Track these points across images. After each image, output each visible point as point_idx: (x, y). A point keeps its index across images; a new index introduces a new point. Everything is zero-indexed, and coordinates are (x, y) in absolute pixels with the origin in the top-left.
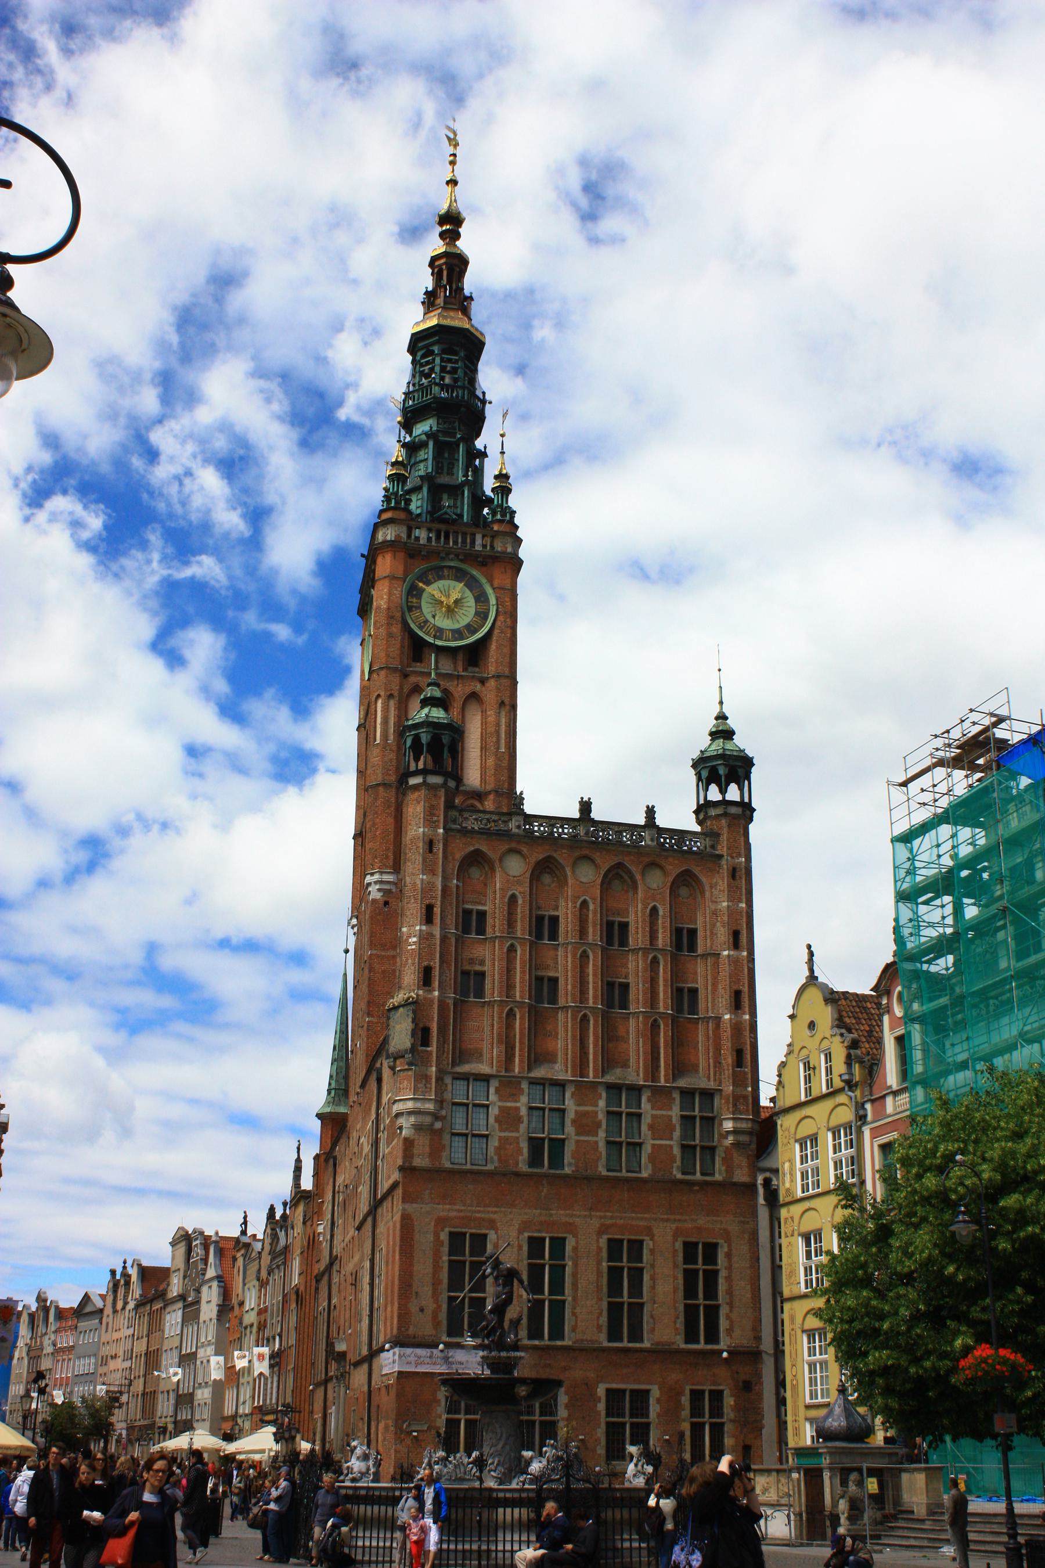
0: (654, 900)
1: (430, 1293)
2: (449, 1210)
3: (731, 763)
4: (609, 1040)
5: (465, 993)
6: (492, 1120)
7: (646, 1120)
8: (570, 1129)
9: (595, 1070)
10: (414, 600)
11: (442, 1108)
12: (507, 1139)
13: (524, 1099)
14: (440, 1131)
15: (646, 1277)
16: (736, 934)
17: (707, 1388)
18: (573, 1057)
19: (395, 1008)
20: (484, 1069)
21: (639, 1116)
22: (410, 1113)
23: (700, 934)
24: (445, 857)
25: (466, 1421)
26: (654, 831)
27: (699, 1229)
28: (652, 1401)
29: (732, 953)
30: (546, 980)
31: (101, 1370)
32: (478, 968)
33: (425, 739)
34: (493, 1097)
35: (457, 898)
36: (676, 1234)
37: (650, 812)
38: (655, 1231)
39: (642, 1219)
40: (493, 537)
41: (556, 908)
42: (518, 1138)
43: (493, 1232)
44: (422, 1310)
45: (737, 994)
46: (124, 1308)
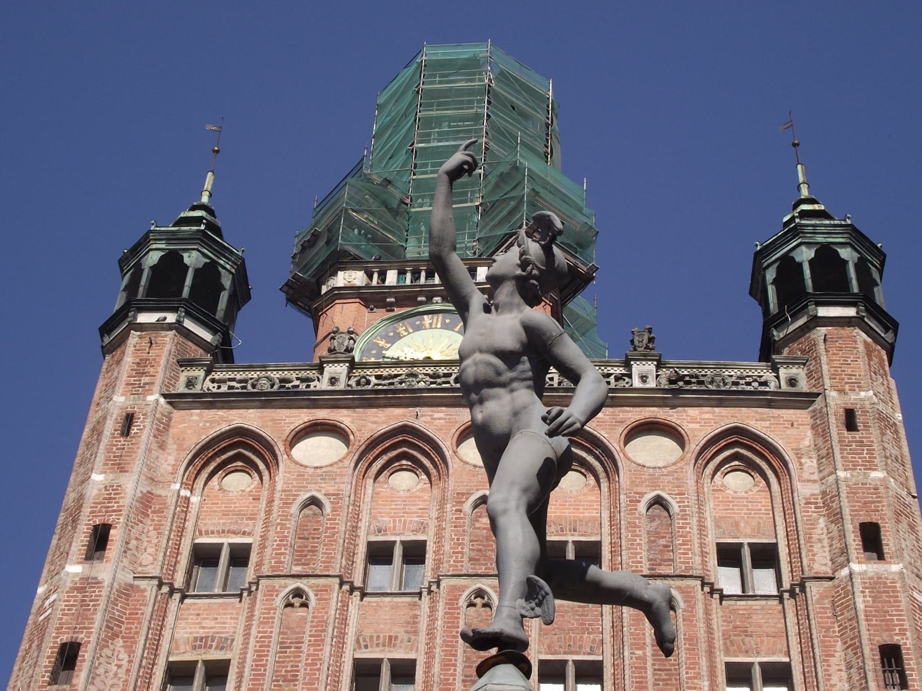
0: (655, 486)
3: (820, 239)
29: (861, 567)
32: (215, 655)
41: (423, 528)
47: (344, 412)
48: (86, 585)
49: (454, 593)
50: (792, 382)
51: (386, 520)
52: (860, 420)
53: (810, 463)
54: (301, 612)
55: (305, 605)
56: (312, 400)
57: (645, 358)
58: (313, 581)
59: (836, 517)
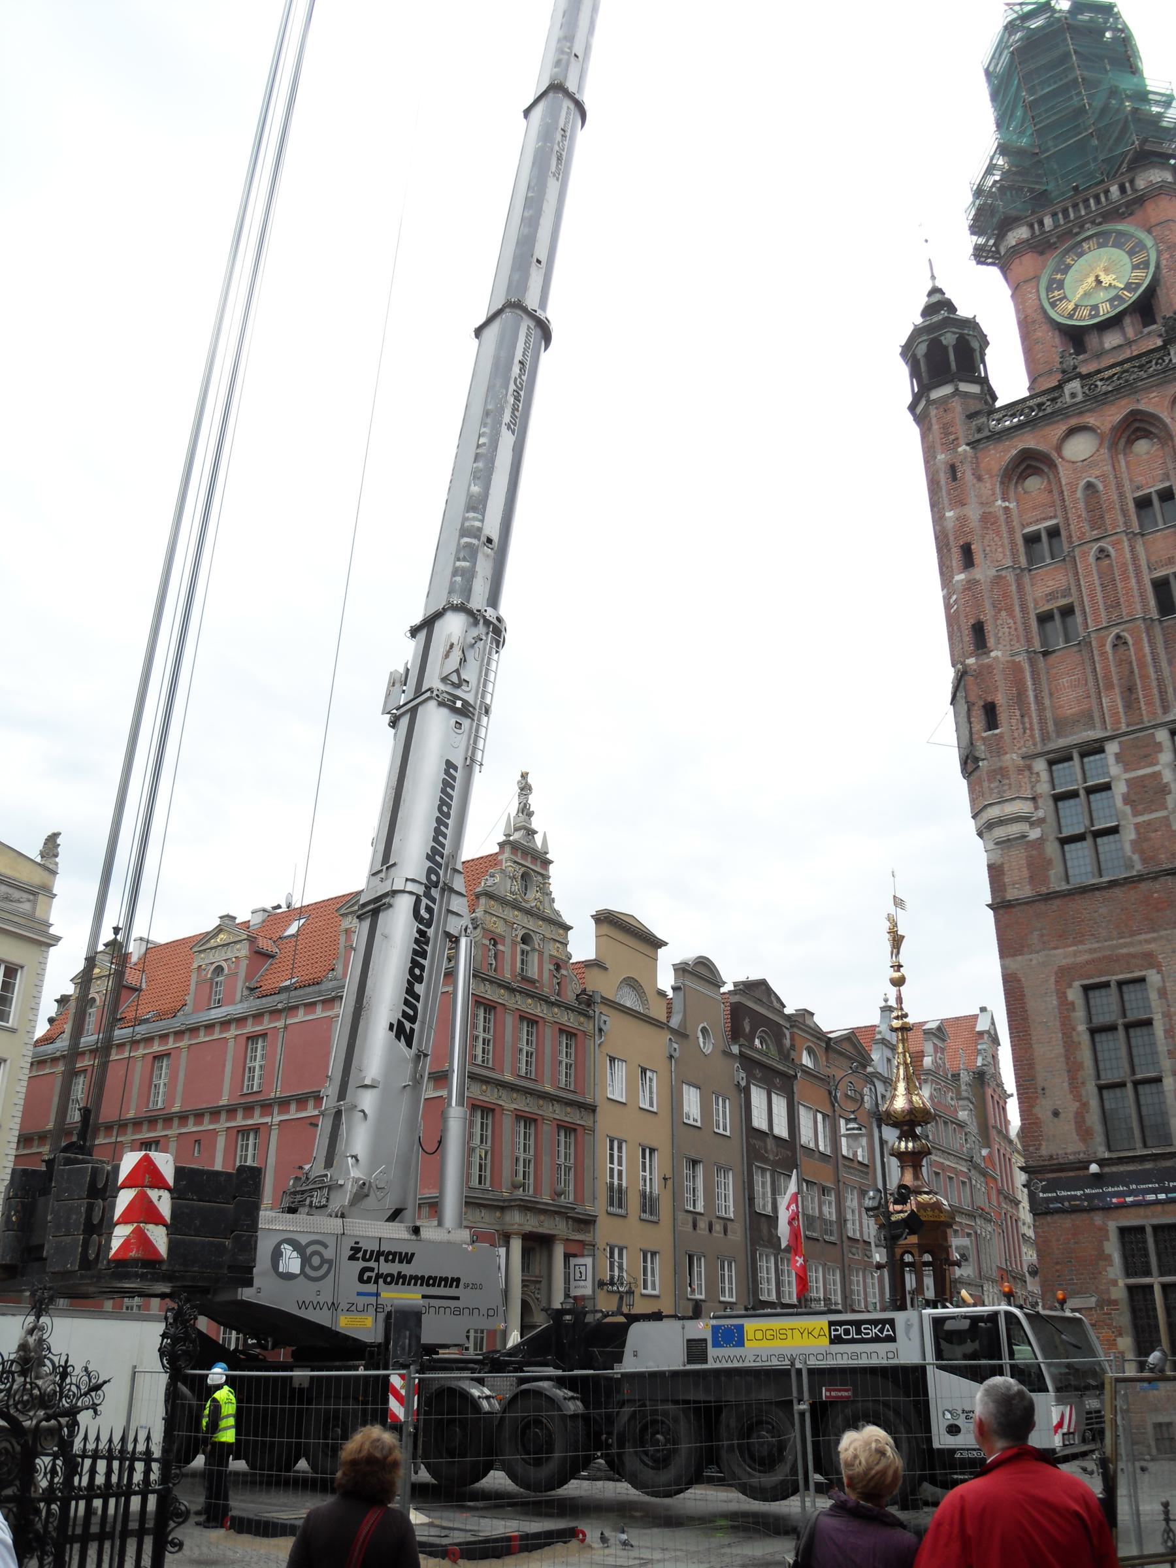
1: (1066, 1084)
2: (1075, 954)
10: (1056, 293)
11: (1036, 808)
12: (1148, 823)
14: (1041, 840)
20: (1097, 734)
24: (980, 479)
25: (1165, 1287)
32: (1063, 602)
35: (1009, 521)
40: (1132, 182)
42: (1166, 818)
43: (1154, 971)
44: (1056, 1114)
47: (1089, 414)
48: (971, 584)
51: (1140, 479)
55: (1108, 556)
56: (1062, 413)
58: (1108, 539)
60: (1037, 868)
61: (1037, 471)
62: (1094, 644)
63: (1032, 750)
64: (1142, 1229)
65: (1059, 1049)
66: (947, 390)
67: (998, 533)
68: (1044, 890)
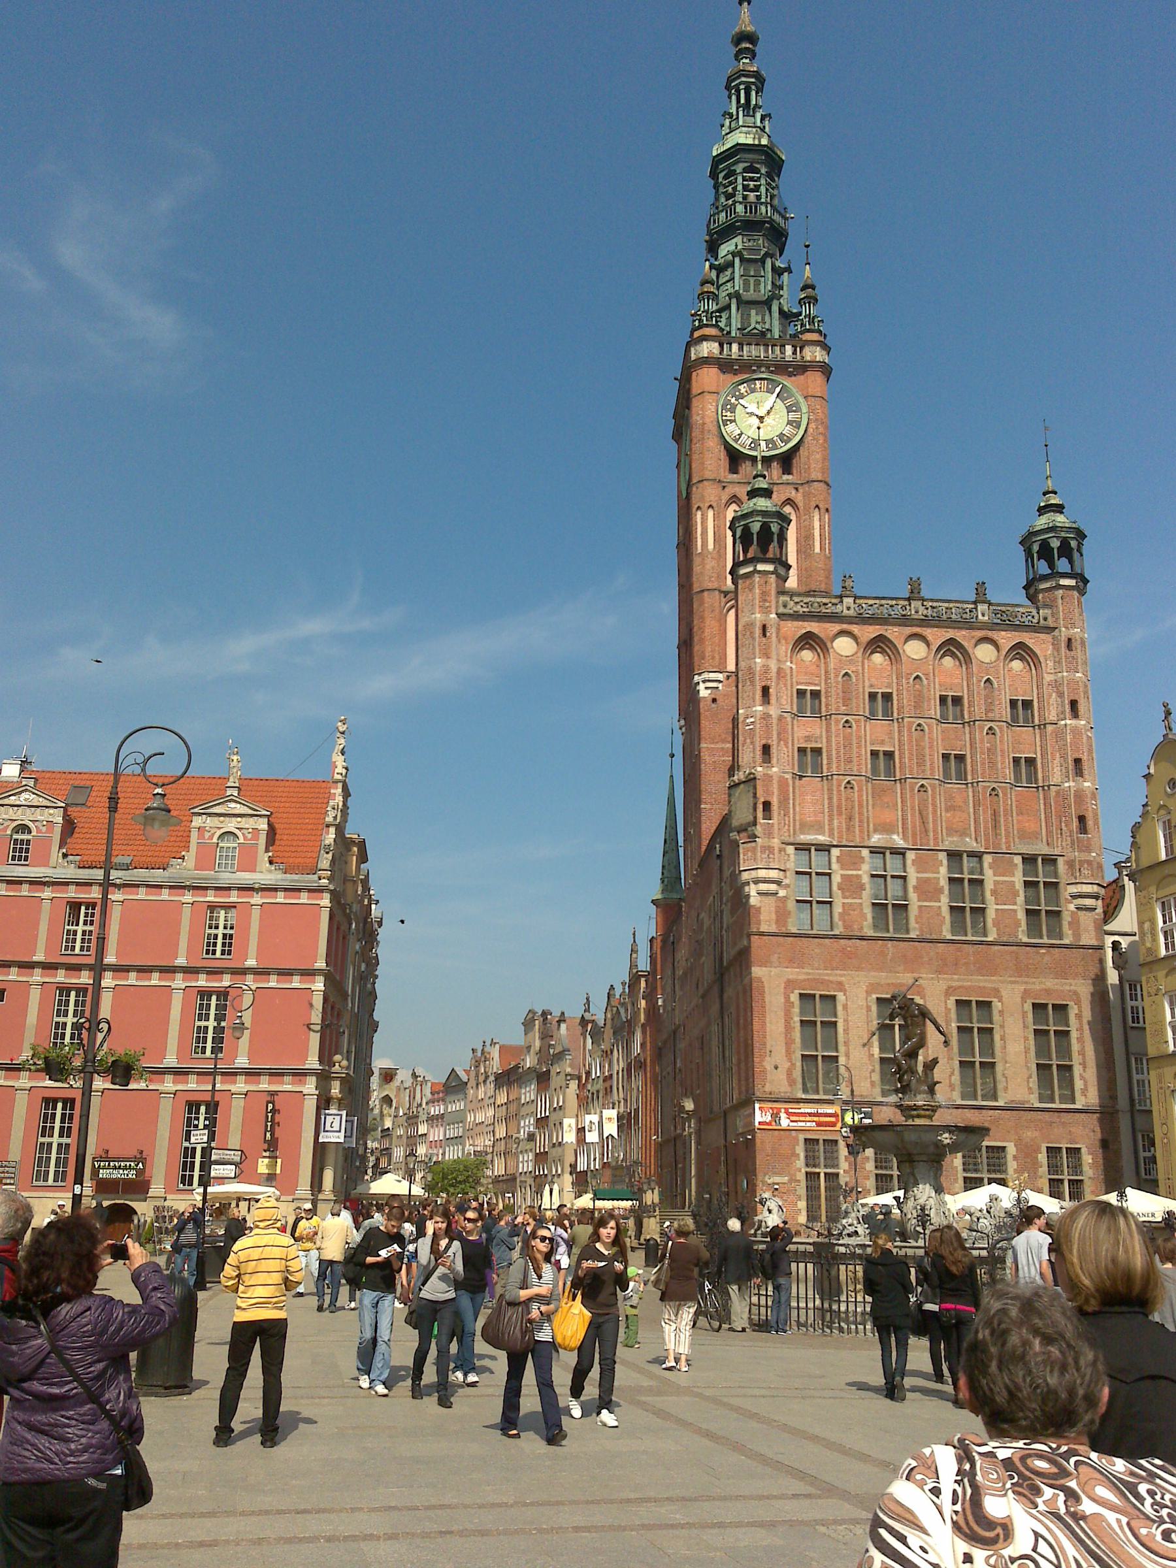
2: (798, 973)
3: (1063, 535)
4: (947, 810)
5: (802, 766)
6: (835, 887)
7: (989, 885)
8: (912, 895)
9: (936, 839)
10: (728, 414)
13: (865, 867)
15: (997, 1037)
16: (1074, 704)
17: (1064, 1146)
18: (914, 827)
19: (737, 785)
21: (981, 882)
22: (757, 881)
23: (1035, 704)
24: (779, 641)
25: (825, 1174)
26: (985, 606)
27: (1048, 992)
28: (1010, 1157)
29: (1068, 722)
30: (881, 755)
31: (468, 1134)
33: (756, 527)
34: (835, 866)
36: (1026, 994)
37: (980, 588)
38: (1003, 993)
39: (990, 981)
45: (1078, 761)
46: (485, 1082)
48: (766, 717)
49: (911, 724)
50: (1045, 619)
52: (1074, 644)
53: (1050, 664)
54: (849, 730)
57: (984, 602)
59: (1061, 695)
60: (782, 915)
61: (812, 648)
62: (835, 782)
63: (787, 839)
64: (818, 1140)
65: (782, 1029)
66: (770, 567)
67: (785, 685)
68: (784, 930)
